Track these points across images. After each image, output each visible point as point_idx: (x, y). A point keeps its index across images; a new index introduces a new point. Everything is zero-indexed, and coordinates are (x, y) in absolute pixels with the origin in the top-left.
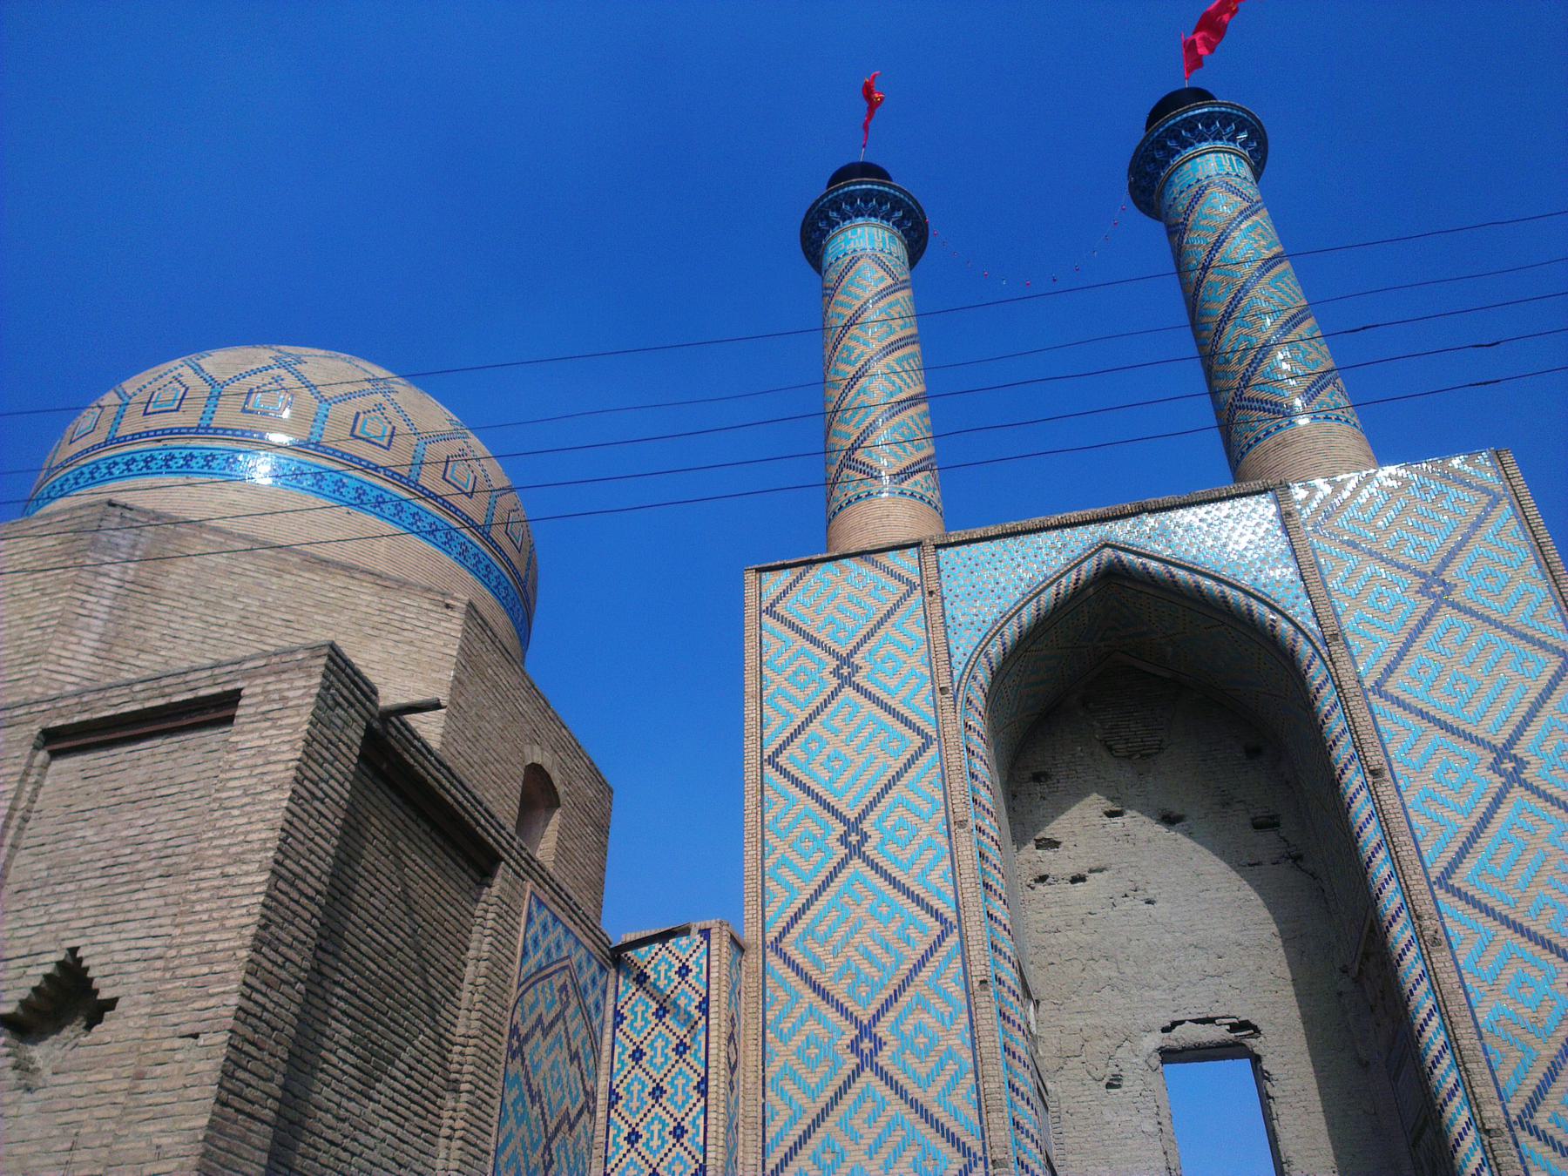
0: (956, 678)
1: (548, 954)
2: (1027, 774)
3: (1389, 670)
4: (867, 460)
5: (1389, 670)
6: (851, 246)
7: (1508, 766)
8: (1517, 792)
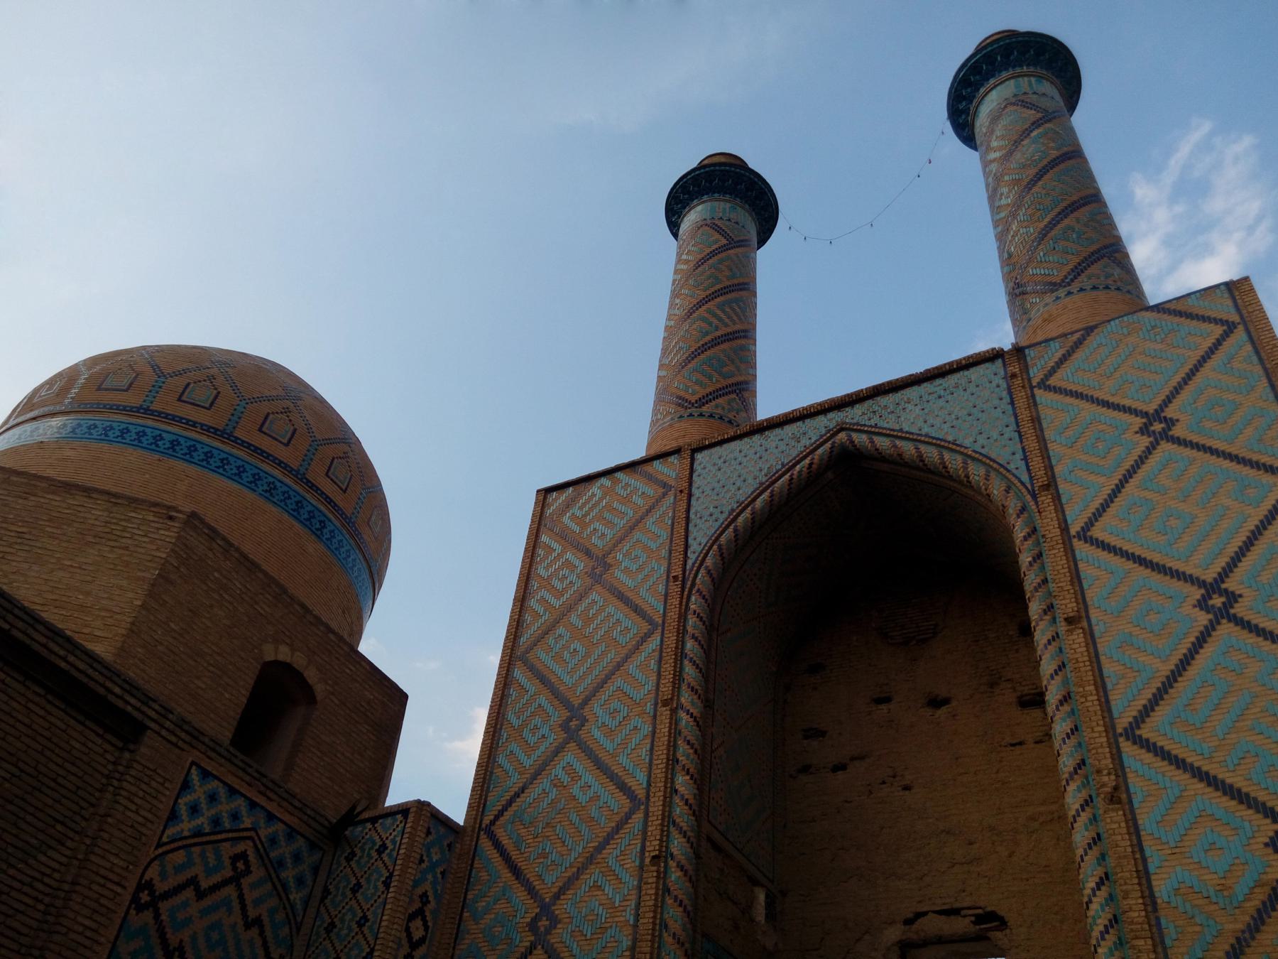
1: (216, 821)
7: (1217, 601)
8: (1226, 628)
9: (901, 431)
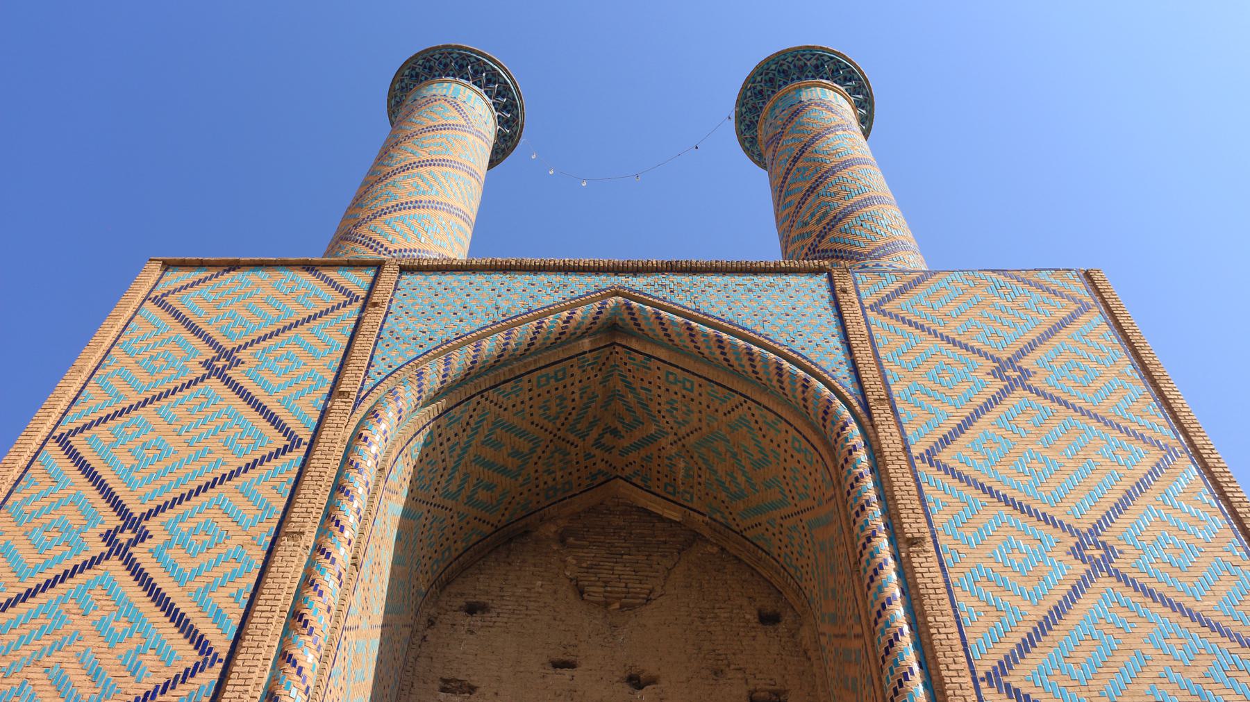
0: (369, 383)
2: (461, 602)
3: (946, 441)
4: (370, 234)
5: (946, 441)
6: (434, 92)
9: (698, 310)
